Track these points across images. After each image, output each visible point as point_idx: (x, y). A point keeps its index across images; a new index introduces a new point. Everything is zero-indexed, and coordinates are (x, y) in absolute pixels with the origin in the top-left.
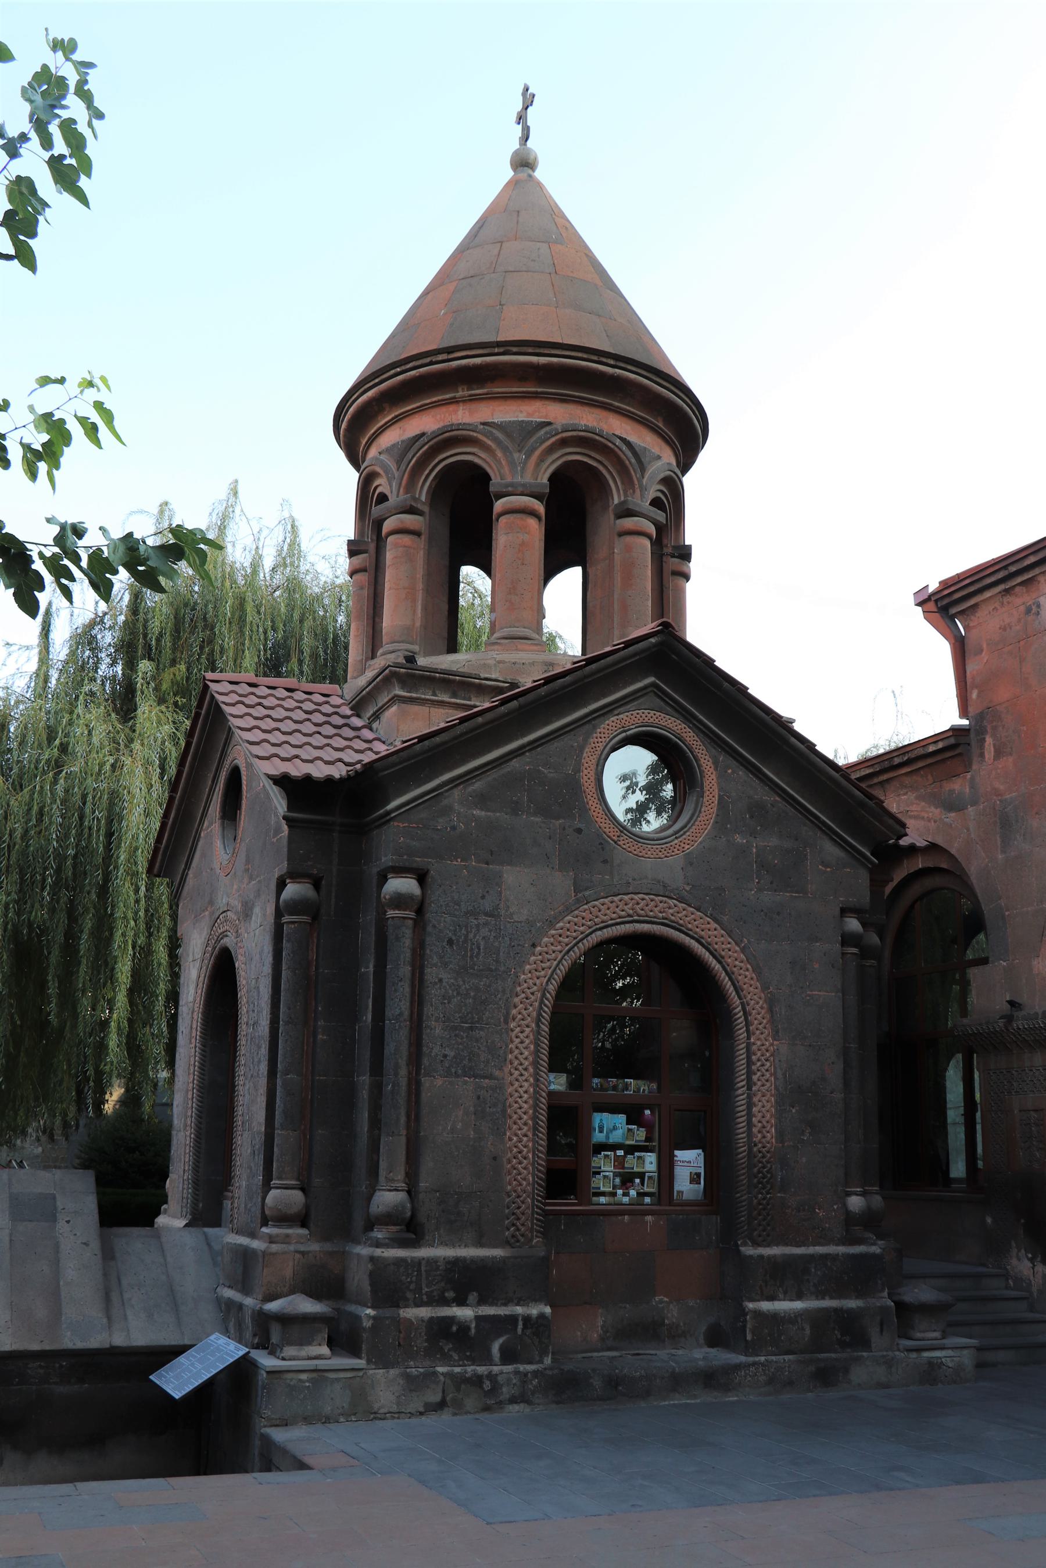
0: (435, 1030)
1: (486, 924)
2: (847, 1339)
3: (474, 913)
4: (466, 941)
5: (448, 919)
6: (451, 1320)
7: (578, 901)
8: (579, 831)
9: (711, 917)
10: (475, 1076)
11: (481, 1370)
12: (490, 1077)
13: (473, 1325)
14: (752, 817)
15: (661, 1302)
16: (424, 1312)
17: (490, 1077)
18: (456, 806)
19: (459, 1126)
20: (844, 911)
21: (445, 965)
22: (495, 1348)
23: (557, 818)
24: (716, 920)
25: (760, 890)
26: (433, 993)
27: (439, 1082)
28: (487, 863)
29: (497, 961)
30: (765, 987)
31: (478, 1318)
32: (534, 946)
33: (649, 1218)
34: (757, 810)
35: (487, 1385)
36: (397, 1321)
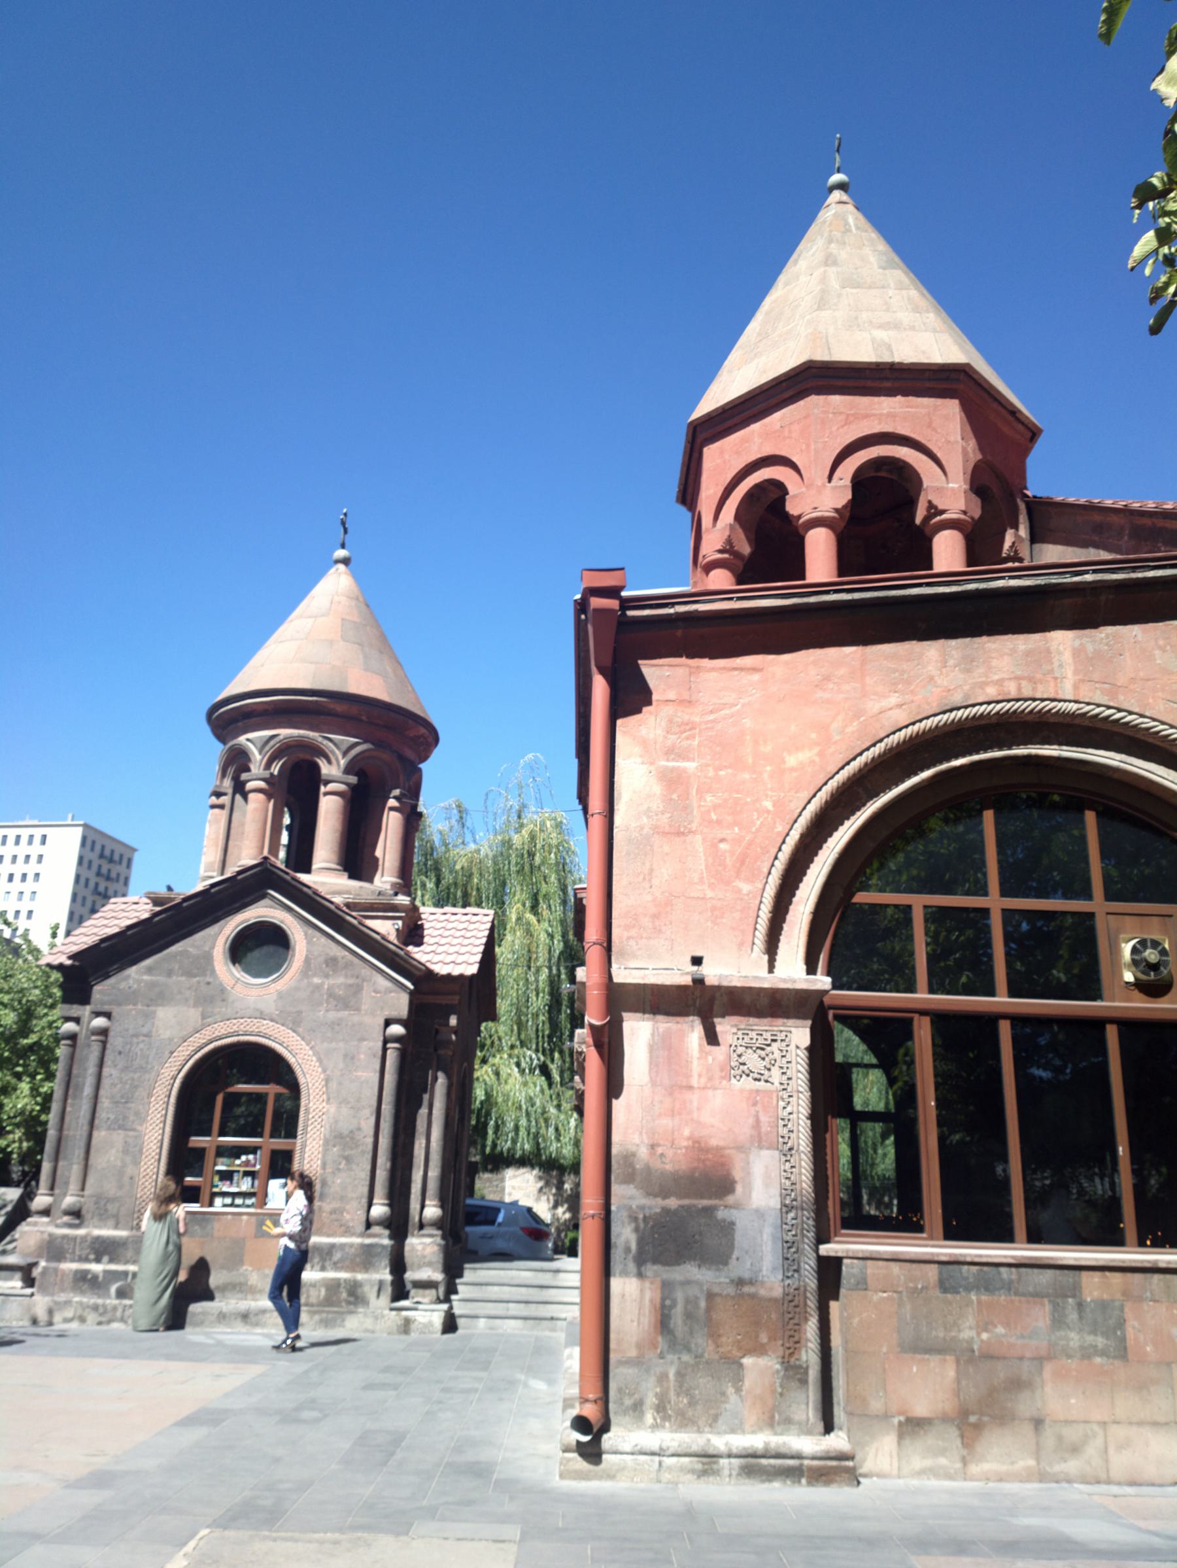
0: (105, 1103)
1: (143, 1041)
2: (352, 1299)
3: (136, 1035)
4: (129, 1051)
5: (120, 1039)
6: (87, 1272)
7: (203, 1025)
8: (208, 983)
9: (291, 1029)
10: (126, 1130)
11: (100, 1301)
12: (134, 1130)
13: (101, 1276)
14: (327, 966)
15: (246, 1270)
16: (75, 1266)
17: (134, 1130)
18: (133, 975)
19: (112, 1159)
20: (388, 1023)
21: (115, 1066)
22: (113, 1289)
23: (195, 976)
24: (294, 1031)
25: (327, 1011)
26: (106, 1082)
27: (103, 1133)
28: (148, 1006)
29: (147, 1063)
30: (324, 1071)
31: (106, 1272)
32: (172, 1053)
33: (245, 1217)
34: (332, 962)
35: (101, 1310)
36: (56, 1270)
